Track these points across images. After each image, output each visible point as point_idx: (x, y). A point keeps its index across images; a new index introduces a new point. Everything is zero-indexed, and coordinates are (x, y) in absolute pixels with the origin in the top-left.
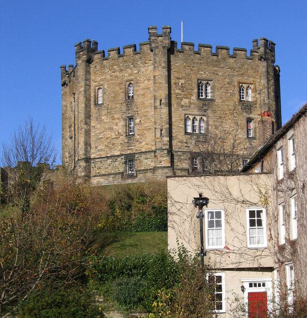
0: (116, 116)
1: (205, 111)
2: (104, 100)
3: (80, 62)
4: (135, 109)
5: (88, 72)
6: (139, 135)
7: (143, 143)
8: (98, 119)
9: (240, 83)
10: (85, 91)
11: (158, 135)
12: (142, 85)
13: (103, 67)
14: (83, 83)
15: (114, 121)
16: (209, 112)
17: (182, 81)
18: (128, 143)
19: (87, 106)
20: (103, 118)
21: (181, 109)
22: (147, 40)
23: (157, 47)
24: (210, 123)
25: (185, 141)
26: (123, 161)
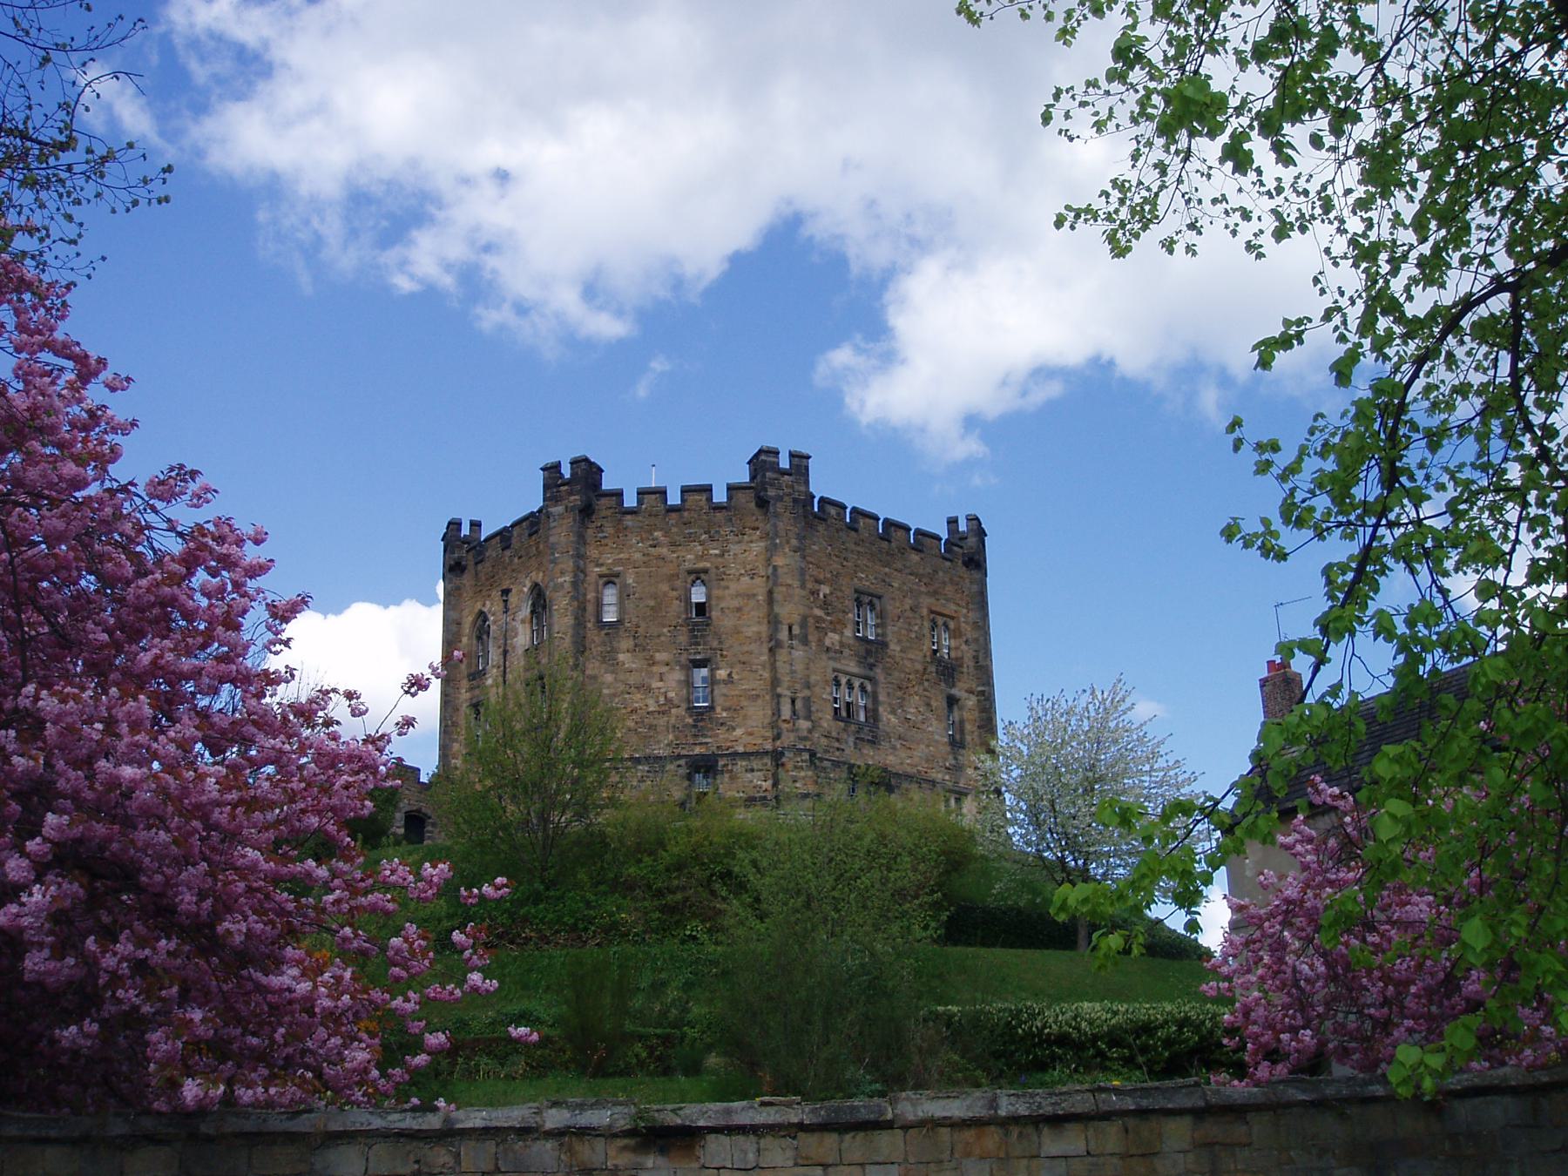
1: (871, 666)
2: (622, 610)
3: (558, 509)
4: (715, 644)
5: (581, 539)
6: (725, 709)
7: (738, 732)
8: (609, 658)
9: (932, 612)
10: (575, 584)
11: (786, 712)
12: (734, 587)
13: (621, 530)
14: (568, 564)
15: (655, 669)
16: (878, 670)
17: (825, 589)
18: (695, 726)
19: (580, 623)
20: (621, 657)
21: (824, 657)
22: (744, 476)
23: (780, 498)
24: (882, 697)
25: (834, 734)
26: (683, 771)
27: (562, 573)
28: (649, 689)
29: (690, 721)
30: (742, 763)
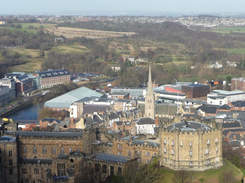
0: (187, 150)
2: (183, 145)
7: (195, 159)
8: (181, 150)
12: (195, 143)
14: (177, 140)
23: (200, 134)
24: (209, 151)
27: (177, 141)
28: (186, 153)
29: (190, 157)
30: (195, 162)
